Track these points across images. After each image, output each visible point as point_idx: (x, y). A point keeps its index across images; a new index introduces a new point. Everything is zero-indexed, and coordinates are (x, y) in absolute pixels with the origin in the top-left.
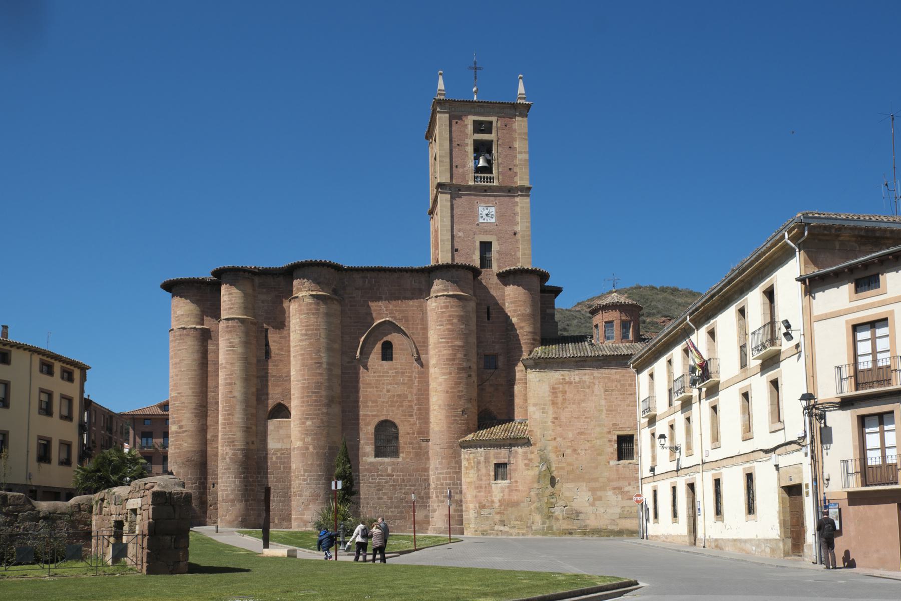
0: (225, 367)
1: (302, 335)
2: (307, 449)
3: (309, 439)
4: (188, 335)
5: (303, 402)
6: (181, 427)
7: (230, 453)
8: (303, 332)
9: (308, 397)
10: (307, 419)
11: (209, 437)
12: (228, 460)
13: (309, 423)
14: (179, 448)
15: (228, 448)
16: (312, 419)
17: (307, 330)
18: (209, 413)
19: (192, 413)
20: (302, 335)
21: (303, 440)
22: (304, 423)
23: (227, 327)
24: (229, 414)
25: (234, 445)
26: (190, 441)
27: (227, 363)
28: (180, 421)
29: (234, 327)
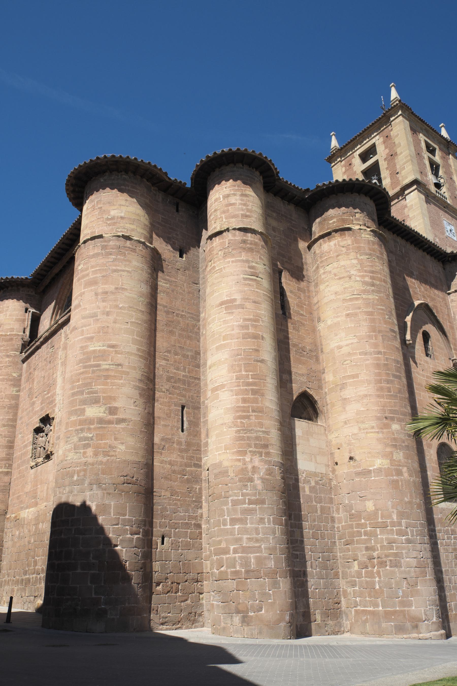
0: (242, 306)
1: (365, 283)
2: (399, 473)
3: (399, 456)
4: (134, 250)
5: (381, 389)
6: (113, 411)
7: (263, 469)
8: (367, 279)
9: (388, 382)
10: (392, 419)
11: (157, 440)
12: (258, 482)
13: (395, 427)
14: (106, 454)
15: (257, 462)
16: (400, 420)
17: (372, 278)
18: (158, 394)
19: (136, 387)
20: (365, 283)
21: (389, 456)
22: (387, 426)
23: (244, 242)
24: (254, 392)
25: (268, 454)
26: (131, 441)
27: (246, 299)
28: (114, 399)
29: (256, 244)
